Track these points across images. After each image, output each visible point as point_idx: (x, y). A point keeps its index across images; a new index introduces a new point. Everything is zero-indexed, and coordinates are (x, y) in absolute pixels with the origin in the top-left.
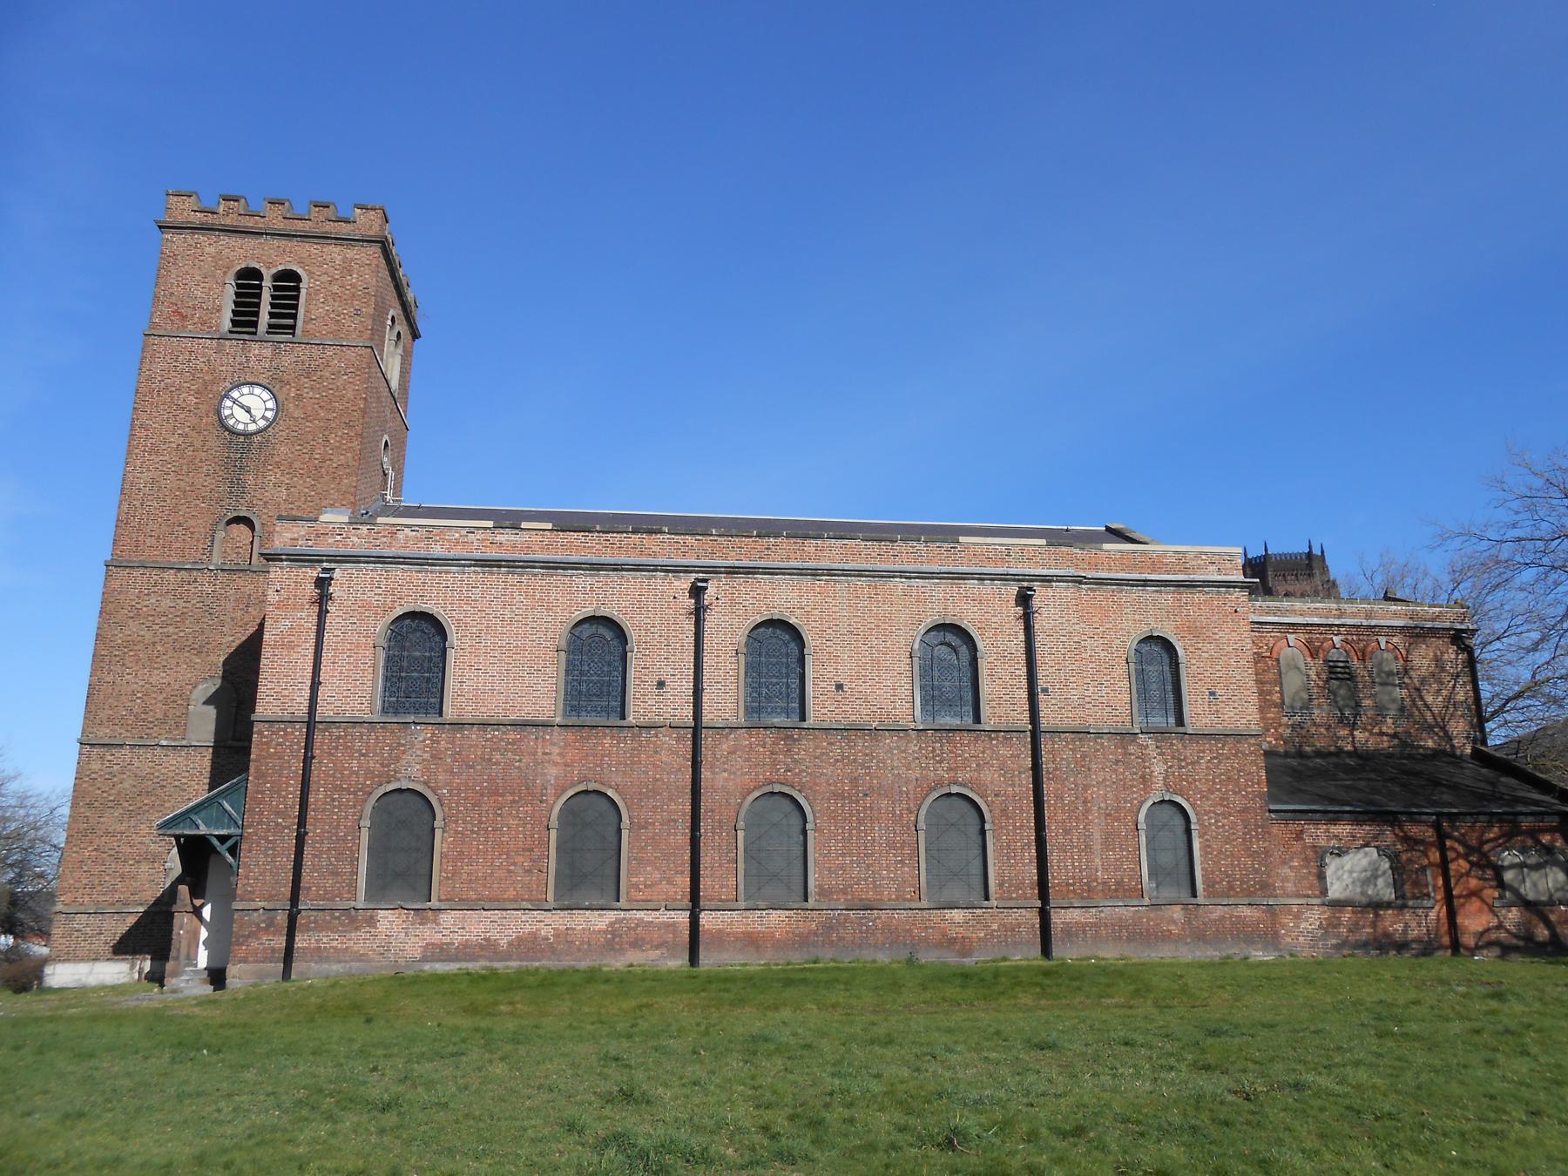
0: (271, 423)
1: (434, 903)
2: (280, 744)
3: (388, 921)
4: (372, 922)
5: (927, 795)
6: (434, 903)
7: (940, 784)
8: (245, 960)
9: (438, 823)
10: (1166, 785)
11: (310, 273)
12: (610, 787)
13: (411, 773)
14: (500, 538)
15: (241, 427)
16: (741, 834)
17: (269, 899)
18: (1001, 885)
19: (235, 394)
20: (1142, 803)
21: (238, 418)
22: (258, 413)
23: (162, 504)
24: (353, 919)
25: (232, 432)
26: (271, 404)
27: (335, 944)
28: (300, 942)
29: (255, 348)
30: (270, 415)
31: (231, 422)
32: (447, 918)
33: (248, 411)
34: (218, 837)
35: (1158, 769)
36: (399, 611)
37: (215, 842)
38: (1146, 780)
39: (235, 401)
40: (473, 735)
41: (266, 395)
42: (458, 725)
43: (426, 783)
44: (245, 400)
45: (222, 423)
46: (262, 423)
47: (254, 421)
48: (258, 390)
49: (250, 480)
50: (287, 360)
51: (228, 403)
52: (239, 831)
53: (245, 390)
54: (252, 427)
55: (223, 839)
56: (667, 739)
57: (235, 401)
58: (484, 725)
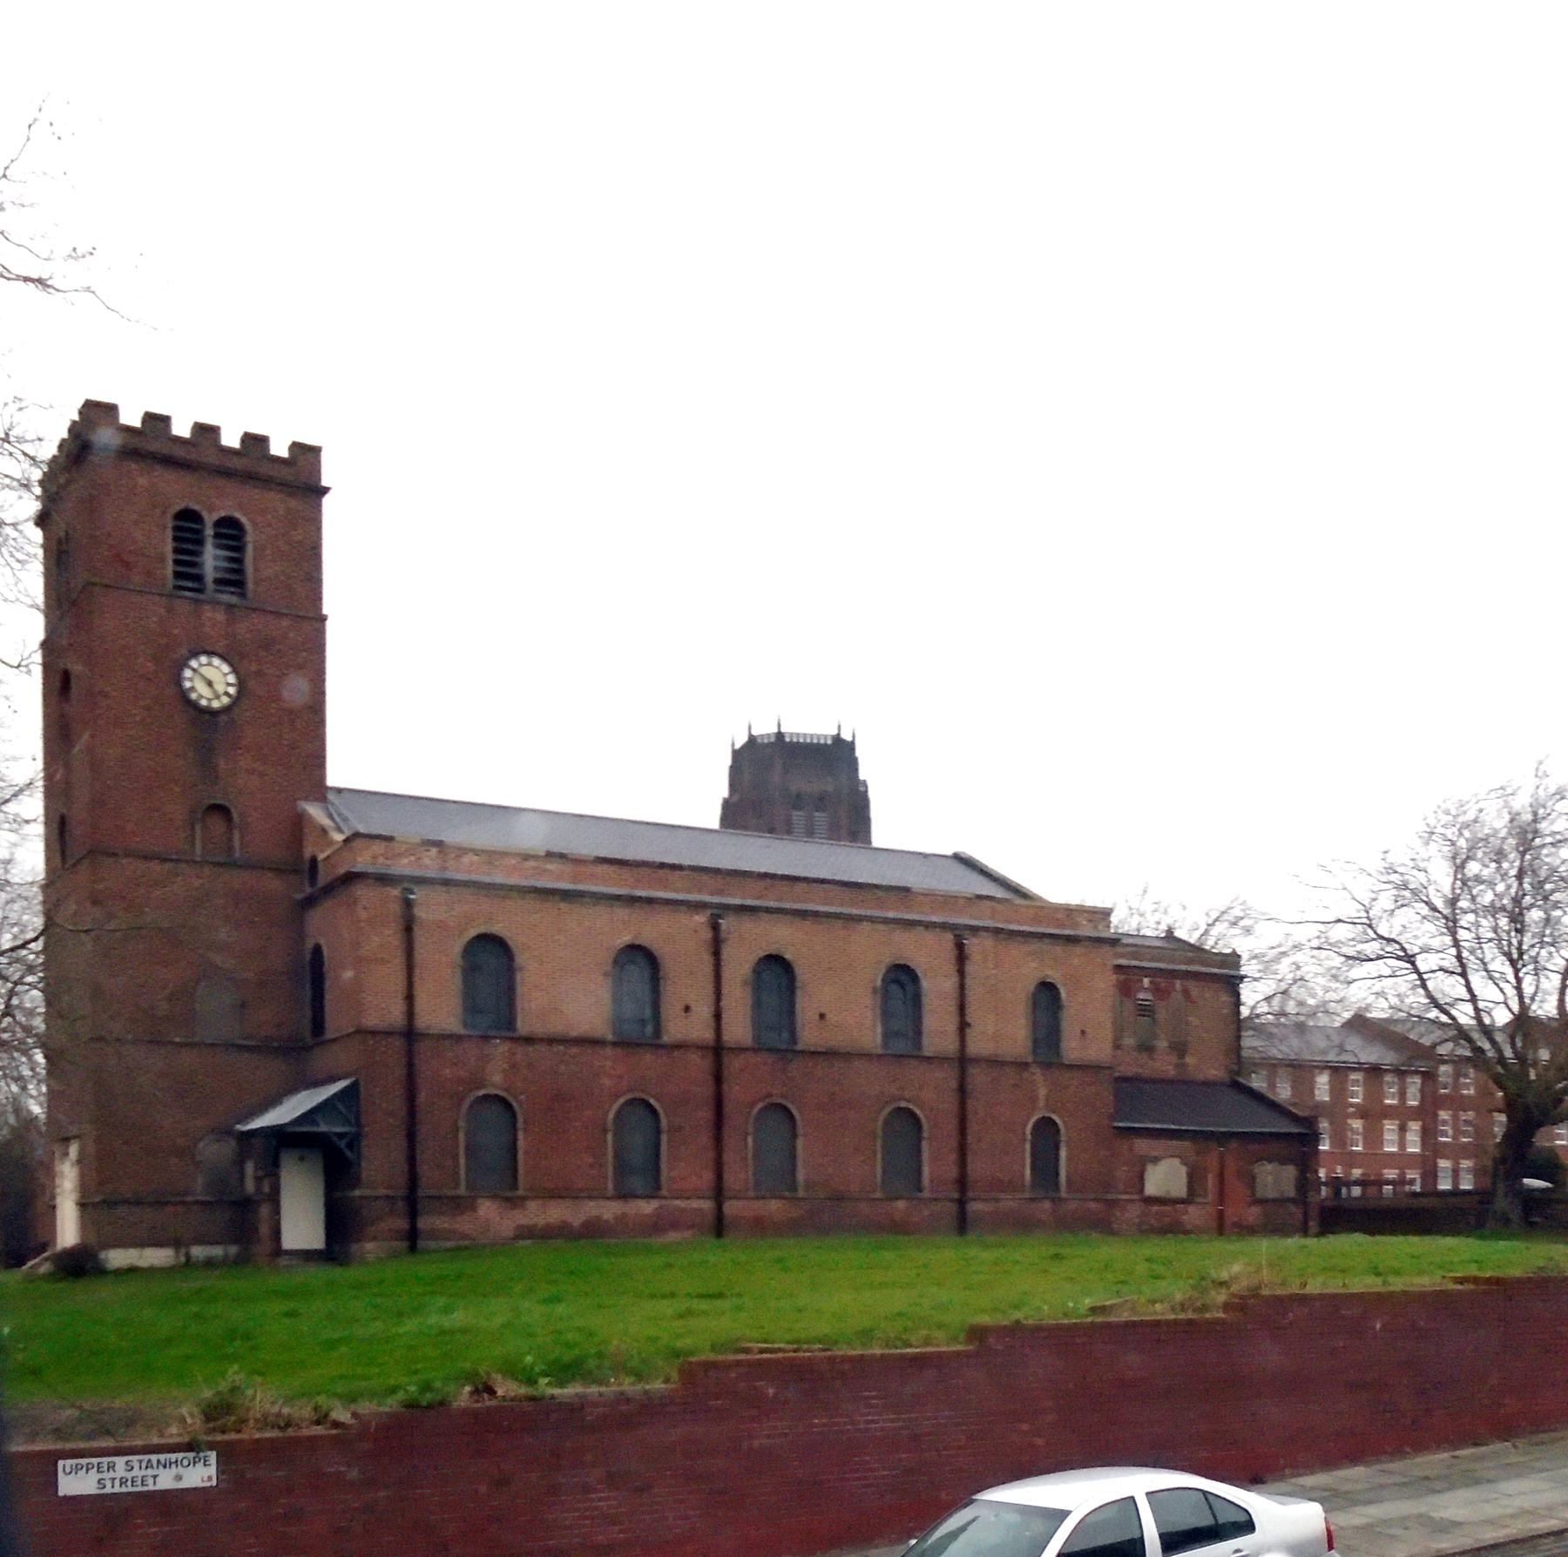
0: (236, 701)
1: (520, 1192)
2: (384, 1052)
3: (487, 1209)
4: (473, 1208)
5: (884, 1107)
6: (520, 1192)
7: (894, 1099)
8: (375, 1238)
9: (520, 1124)
10: (1047, 1106)
11: (255, 524)
12: (652, 1096)
13: (496, 1080)
14: (549, 866)
15: (204, 702)
16: (750, 1139)
17: (389, 1187)
18: (932, 1181)
19: (194, 663)
20: (1029, 1119)
21: (201, 693)
22: (220, 688)
23: (135, 785)
24: (461, 1205)
25: (194, 705)
26: (232, 679)
27: (446, 1225)
28: (423, 1223)
29: (208, 612)
30: (232, 690)
31: (193, 696)
32: (532, 1205)
33: (210, 684)
34: (337, 1134)
35: (1042, 1092)
36: (473, 933)
37: (335, 1139)
38: (1033, 1099)
39: (194, 670)
40: (543, 1048)
41: (226, 668)
42: (529, 1040)
43: (506, 1090)
44: (205, 671)
45: (184, 697)
46: (225, 700)
47: (218, 697)
48: (216, 661)
49: (222, 764)
50: (242, 628)
51: (188, 673)
52: (353, 1130)
53: (204, 659)
54: (216, 704)
55: (341, 1136)
56: (694, 1057)
57: (194, 670)
58: (551, 1041)
